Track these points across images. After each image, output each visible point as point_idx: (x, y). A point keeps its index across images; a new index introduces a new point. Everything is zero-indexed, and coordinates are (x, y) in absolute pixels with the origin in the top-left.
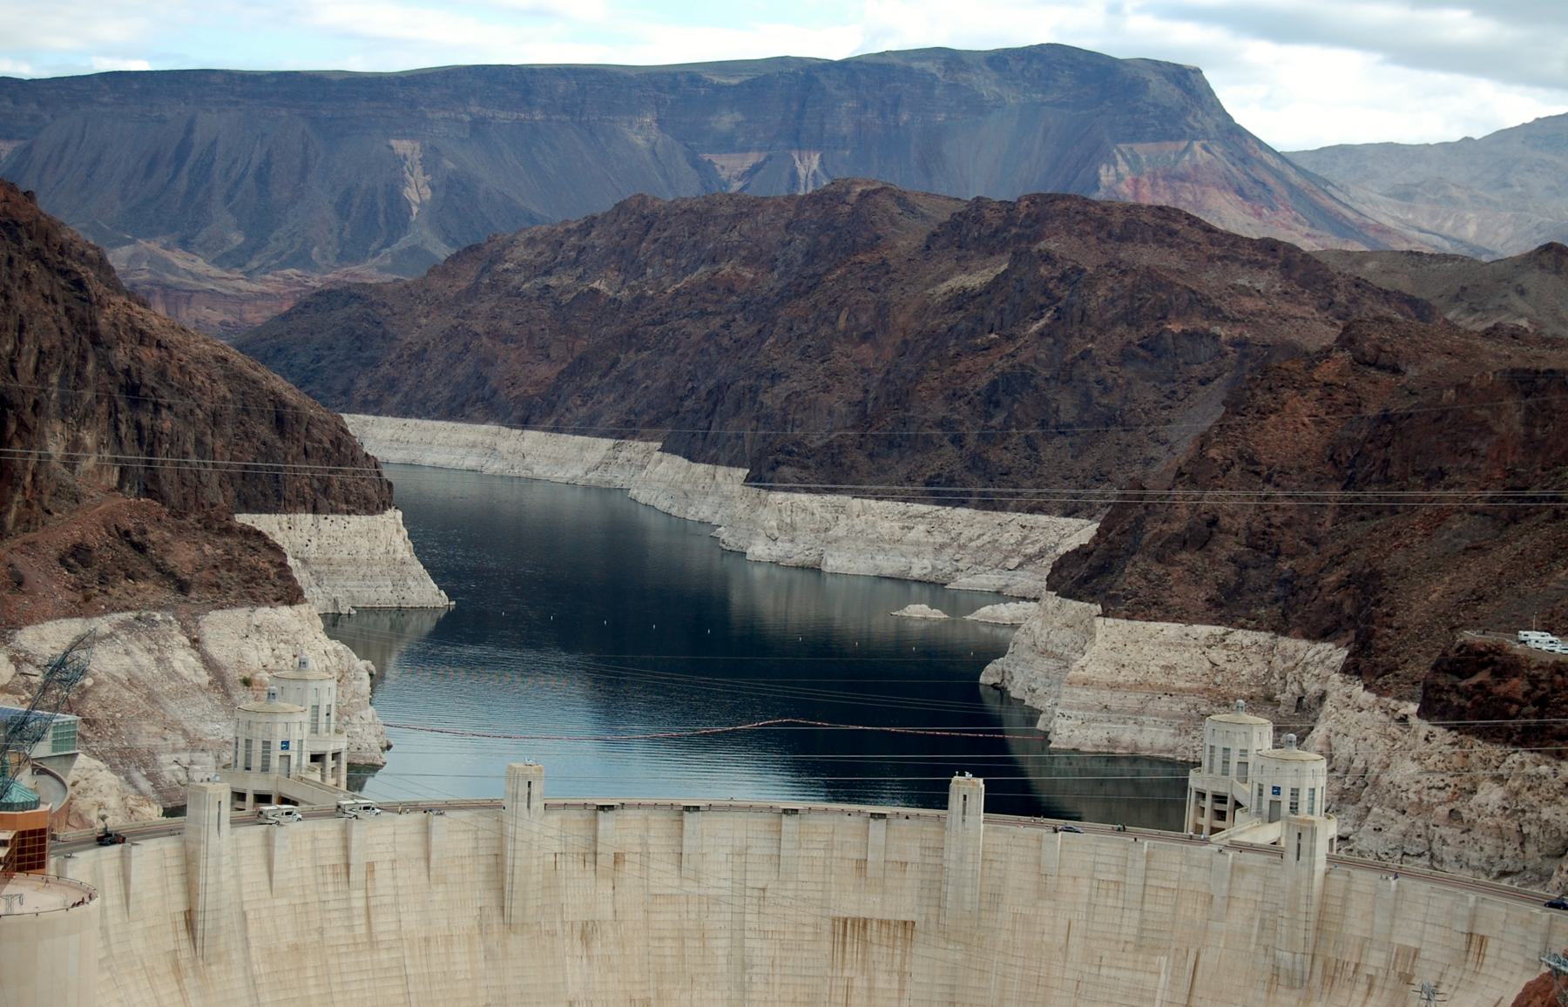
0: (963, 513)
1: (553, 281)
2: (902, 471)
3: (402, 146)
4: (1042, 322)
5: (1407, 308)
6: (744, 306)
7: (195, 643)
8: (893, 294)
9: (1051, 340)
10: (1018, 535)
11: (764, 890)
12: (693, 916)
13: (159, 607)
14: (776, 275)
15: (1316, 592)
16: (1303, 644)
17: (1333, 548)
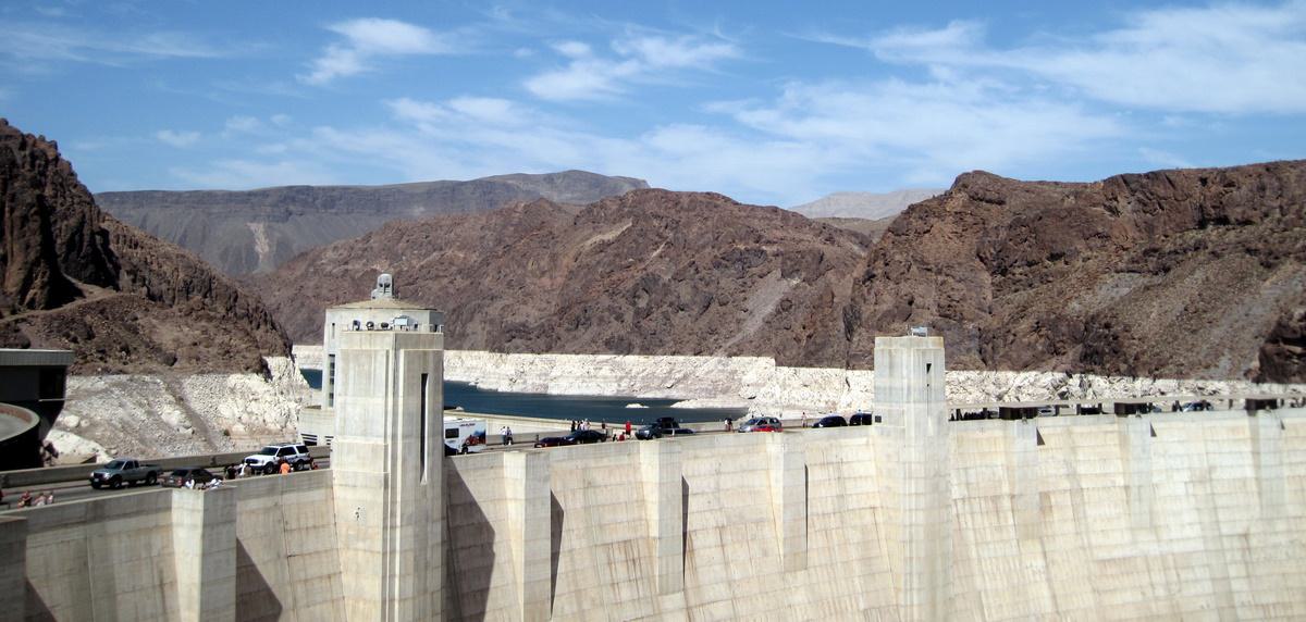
0: (631, 359)
1: (350, 267)
2: (587, 337)
3: (253, 226)
4: (658, 251)
5: (853, 239)
6: (460, 272)
7: (180, 401)
8: (559, 249)
9: (667, 259)
10: (668, 368)
11: (1246, 536)
12: (1161, 592)
13: (150, 372)
14: (477, 254)
15: (1011, 338)
16: (1011, 374)
17: (1006, 312)
